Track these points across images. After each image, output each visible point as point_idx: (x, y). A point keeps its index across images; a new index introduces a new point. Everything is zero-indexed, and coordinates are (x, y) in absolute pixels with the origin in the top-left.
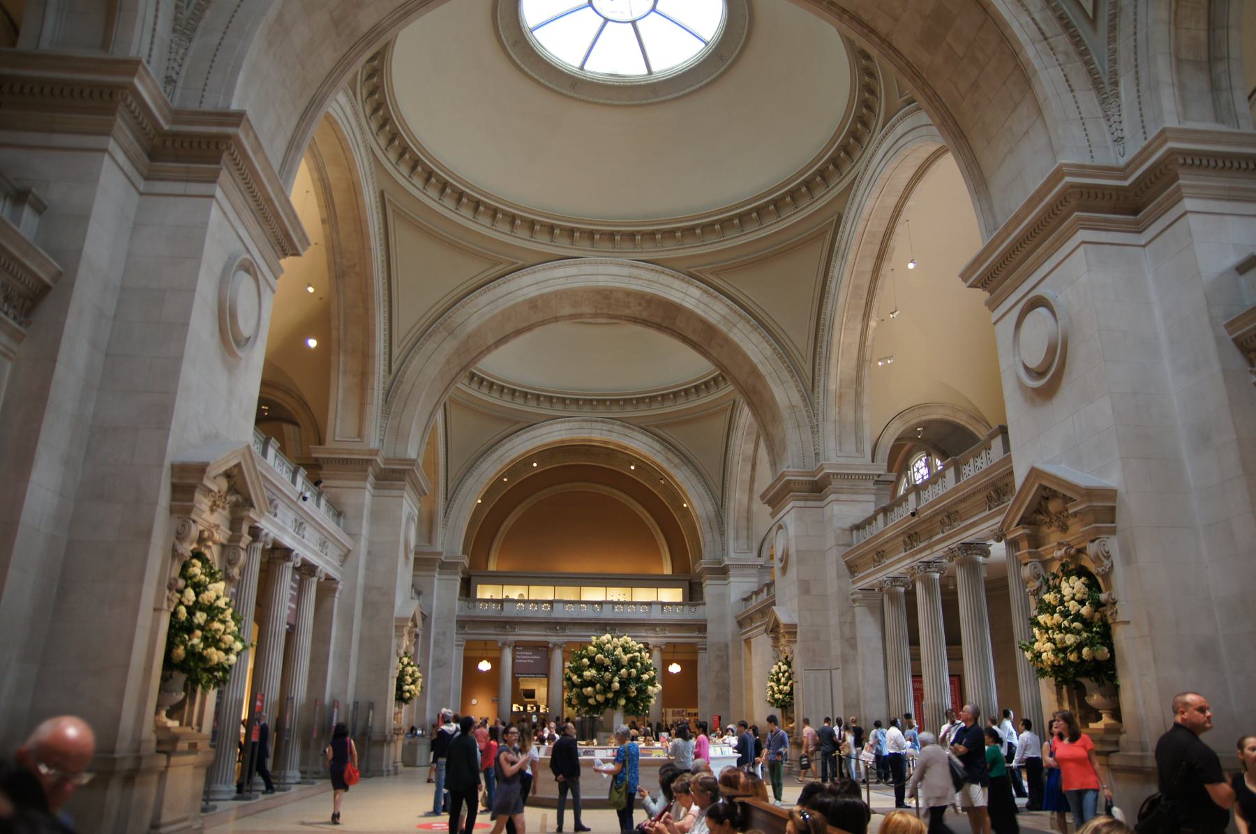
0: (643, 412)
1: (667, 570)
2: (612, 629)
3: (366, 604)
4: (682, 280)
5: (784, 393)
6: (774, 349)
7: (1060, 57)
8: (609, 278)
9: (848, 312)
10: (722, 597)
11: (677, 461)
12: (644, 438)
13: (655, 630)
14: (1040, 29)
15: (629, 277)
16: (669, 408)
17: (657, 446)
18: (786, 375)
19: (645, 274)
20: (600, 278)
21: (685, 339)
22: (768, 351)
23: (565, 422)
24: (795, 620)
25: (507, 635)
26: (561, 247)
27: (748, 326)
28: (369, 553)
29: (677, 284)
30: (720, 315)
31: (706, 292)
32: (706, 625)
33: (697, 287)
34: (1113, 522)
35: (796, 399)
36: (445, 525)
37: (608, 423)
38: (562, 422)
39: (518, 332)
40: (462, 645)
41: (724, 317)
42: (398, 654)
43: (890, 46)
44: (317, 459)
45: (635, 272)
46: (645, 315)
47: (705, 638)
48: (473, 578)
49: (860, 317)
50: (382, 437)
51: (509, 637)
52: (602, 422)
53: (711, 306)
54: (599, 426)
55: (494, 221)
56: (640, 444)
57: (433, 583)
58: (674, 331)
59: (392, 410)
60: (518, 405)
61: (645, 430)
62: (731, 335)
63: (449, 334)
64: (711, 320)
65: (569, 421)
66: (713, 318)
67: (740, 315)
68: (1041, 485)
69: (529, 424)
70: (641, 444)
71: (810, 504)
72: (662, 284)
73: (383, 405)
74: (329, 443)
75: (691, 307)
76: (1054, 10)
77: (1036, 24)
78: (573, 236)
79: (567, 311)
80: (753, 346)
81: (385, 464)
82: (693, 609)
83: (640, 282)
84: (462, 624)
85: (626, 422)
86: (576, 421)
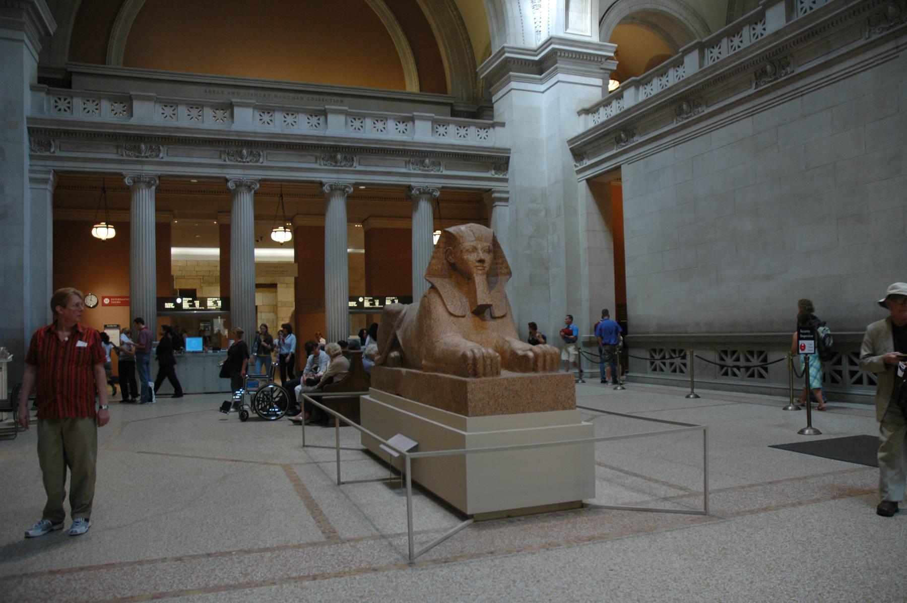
2: (345, 159)
13: (422, 163)
25: (142, 163)
40: (45, 181)
47: (506, 180)
51: (146, 167)
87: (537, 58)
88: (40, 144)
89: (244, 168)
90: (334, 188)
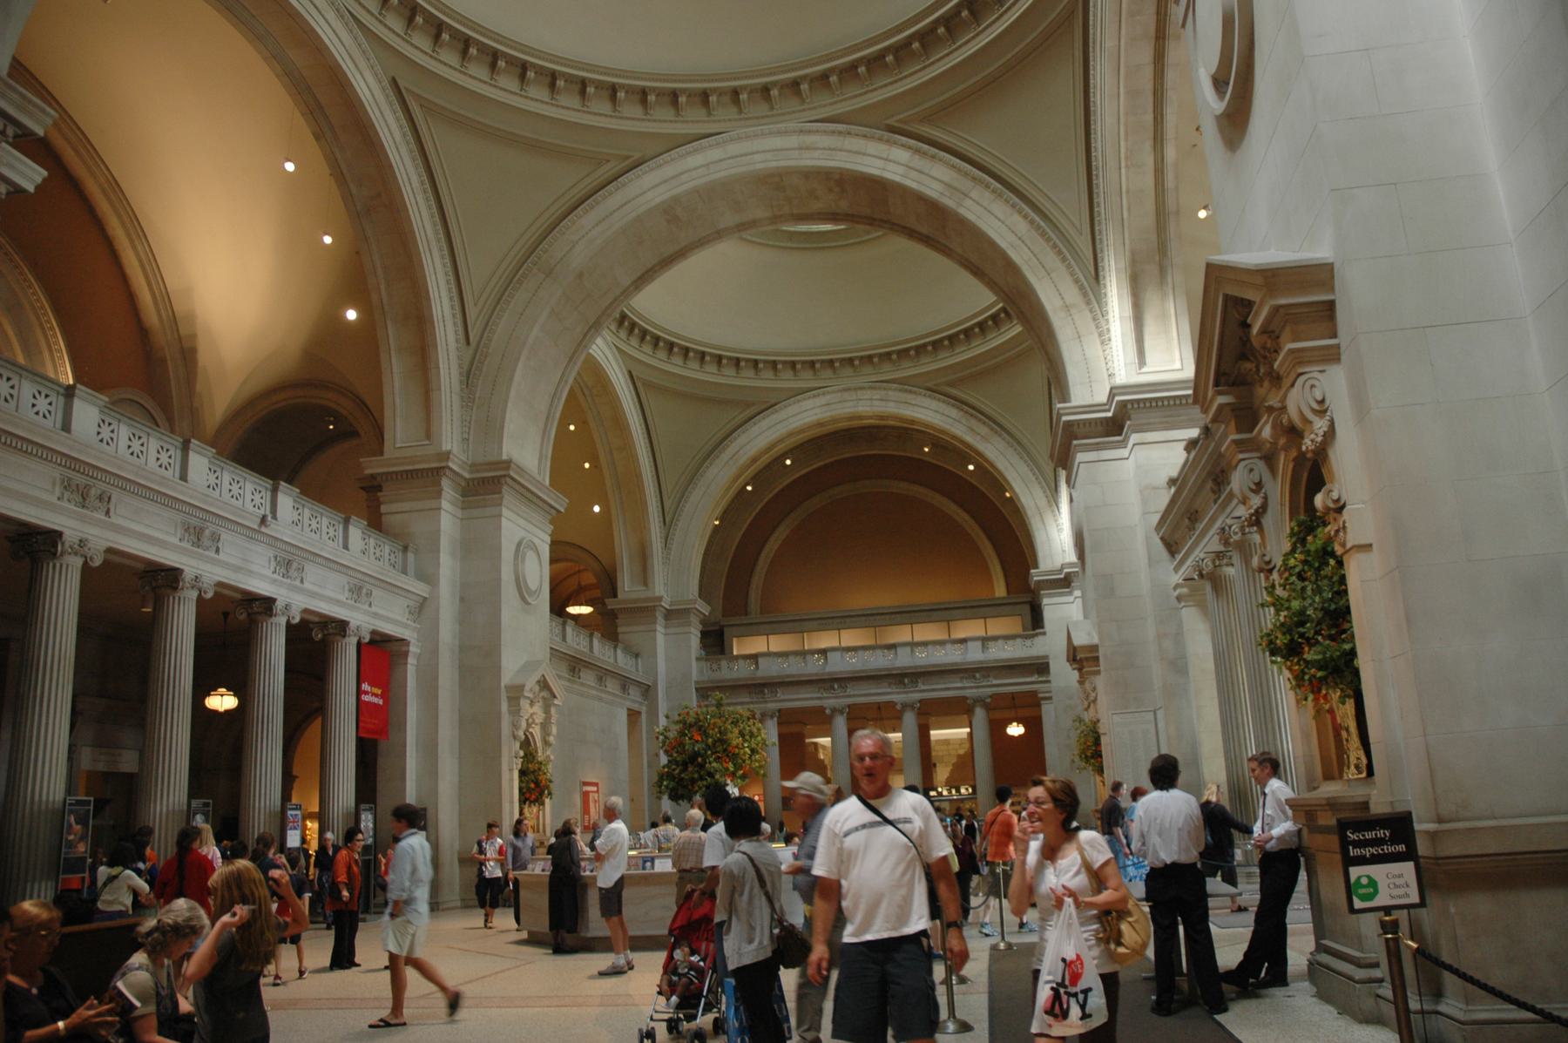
0: (928, 365)
1: (1000, 591)
4: (880, 139)
9: (1126, 140)
11: (984, 430)
12: (934, 404)
13: (974, 677)
15: (800, 149)
16: (964, 354)
17: (954, 413)
18: (1051, 259)
20: (757, 157)
21: (912, 234)
22: (1022, 226)
23: (819, 395)
24: (1096, 641)
25: (766, 702)
26: (692, 121)
27: (987, 194)
29: (873, 147)
30: (942, 182)
31: (917, 151)
32: (1048, 664)
33: (903, 145)
34: (1335, 336)
37: (880, 388)
38: (814, 396)
39: (667, 262)
42: (515, 737)
44: (373, 477)
45: (809, 139)
46: (843, 206)
47: (1049, 682)
48: (725, 629)
50: (466, 436)
52: (870, 388)
53: (927, 171)
54: (868, 394)
55: (584, 99)
56: (929, 412)
57: (655, 639)
58: (894, 224)
59: (477, 395)
60: (747, 379)
61: (934, 391)
62: (962, 211)
63: (547, 276)
64: (929, 192)
65: (824, 394)
66: (932, 190)
67: (974, 179)
68: (1226, 297)
69: (766, 405)
70: (931, 413)
72: (849, 151)
73: (462, 390)
75: (897, 179)
78: (708, 102)
79: (729, 219)
81: (471, 472)
82: (1028, 642)
83: (816, 154)
85: (905, 384)
86: (834, 392)
87: (1062, 576)
88: (703, 696)
89: (836, 697)
90: (905, 706)
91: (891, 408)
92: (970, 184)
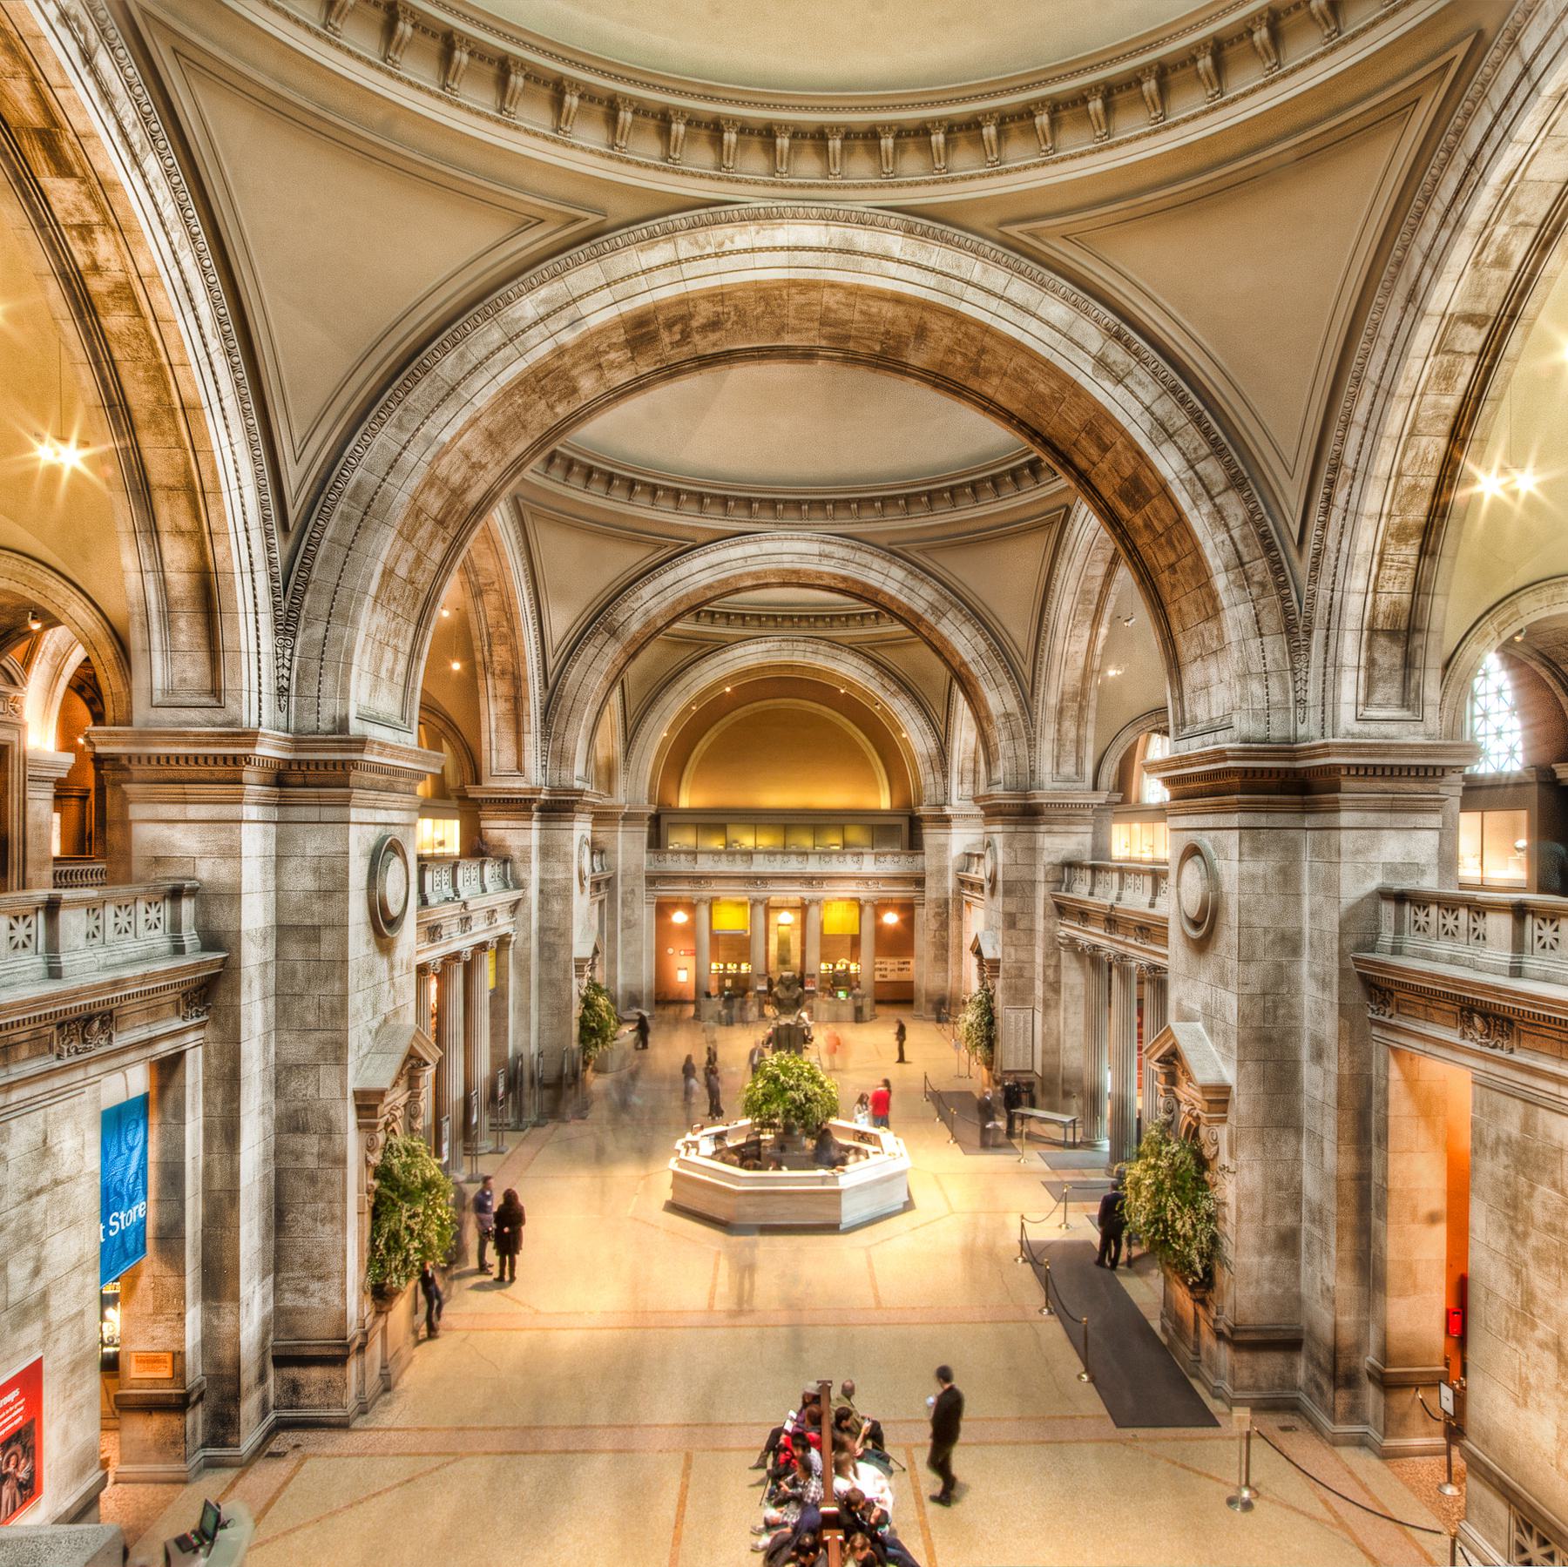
3: (543, 945)
5: (999, 700)
6: (990, 645)
7: (1255, 590)
8: (795, 558)
10: (943, 849)
11: (894, 688)
14: (1237, 551)
17: (871, 670)
18: (1001, 676)
19: (840, 552)
20: (785, 557)
22: (983, 647)
24: (999, 956)
28: (541, 892)
29: (877, 563)
31: (911, 573)
35: (1012, 705)
36: (627, 769)
41: (932, 605)
43: (1088, 482)
45: (828, 548)
49: (1089, 623)
54: (802, 646)
56: (850, 670)
62: (939, 627)
69: (721, 645)
71: (1020, 828)
74: (489, 783)
75: (893, 593)
76: (1260, 524)
77: (1234, 544)
80: (964, 641)
83: (833, 562)
84: (652, 880)
85: (833, 643)
91: (820, 662)
92: (948, 606)
